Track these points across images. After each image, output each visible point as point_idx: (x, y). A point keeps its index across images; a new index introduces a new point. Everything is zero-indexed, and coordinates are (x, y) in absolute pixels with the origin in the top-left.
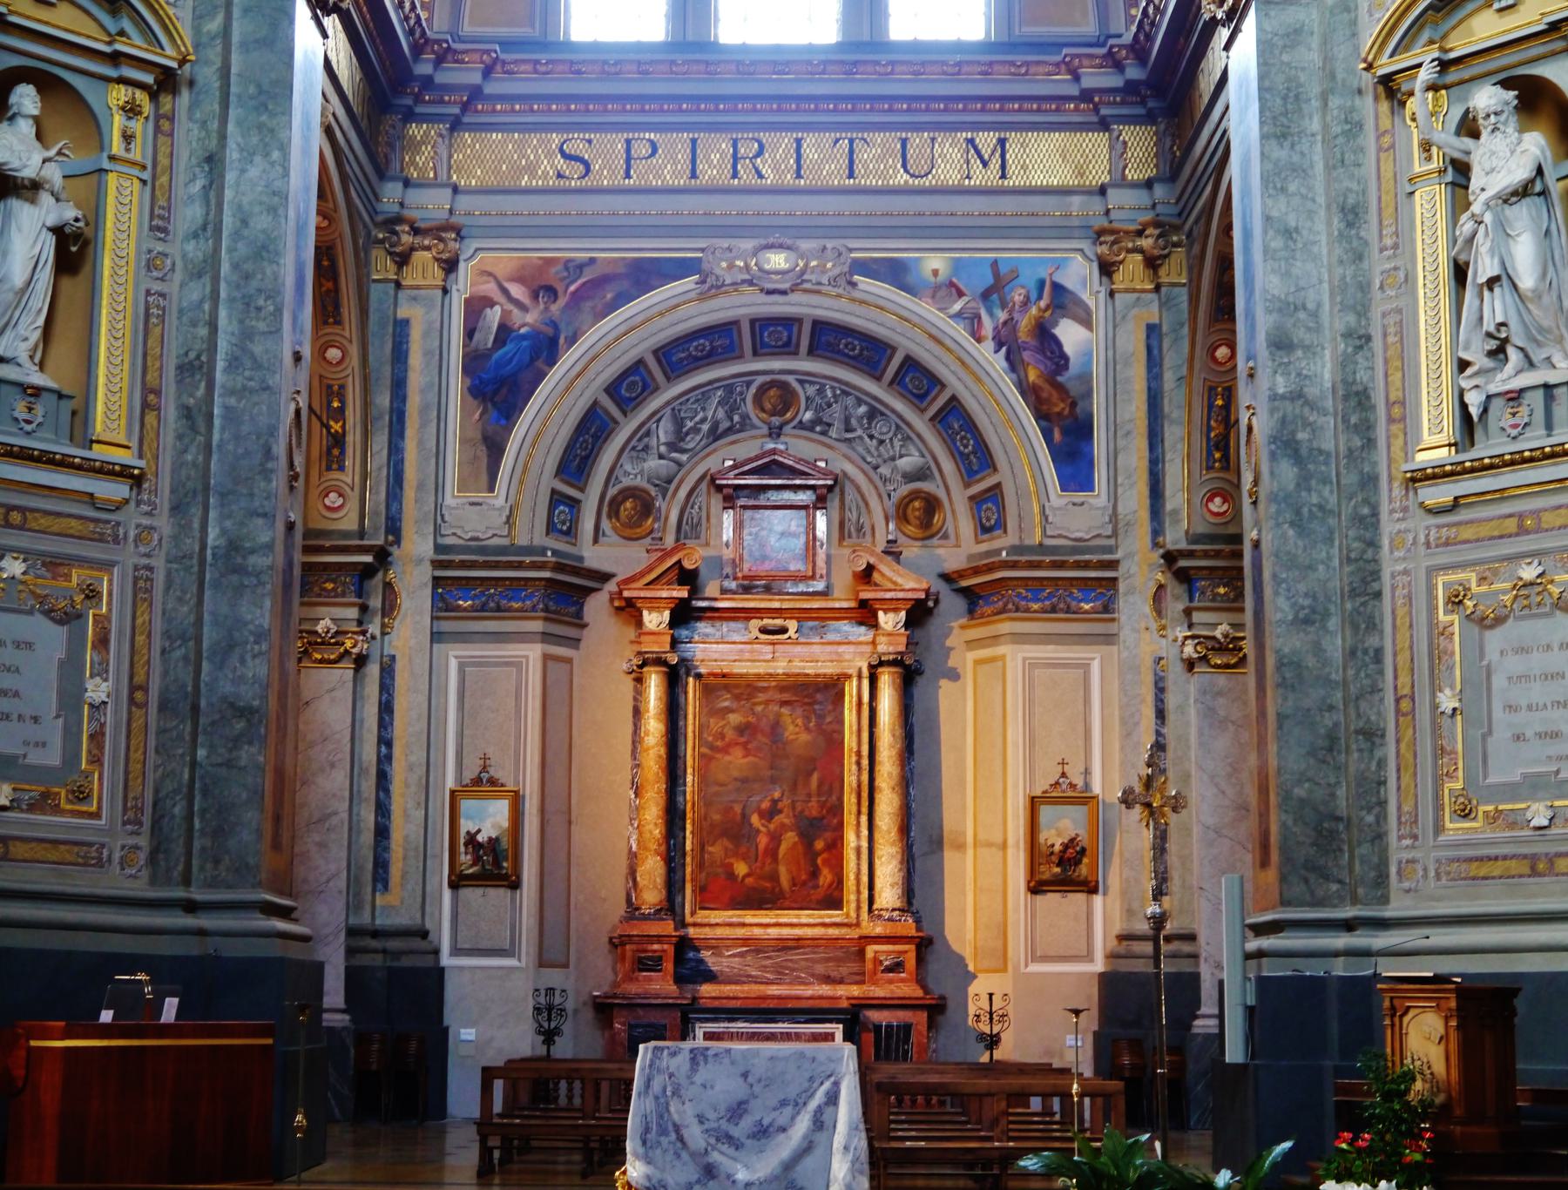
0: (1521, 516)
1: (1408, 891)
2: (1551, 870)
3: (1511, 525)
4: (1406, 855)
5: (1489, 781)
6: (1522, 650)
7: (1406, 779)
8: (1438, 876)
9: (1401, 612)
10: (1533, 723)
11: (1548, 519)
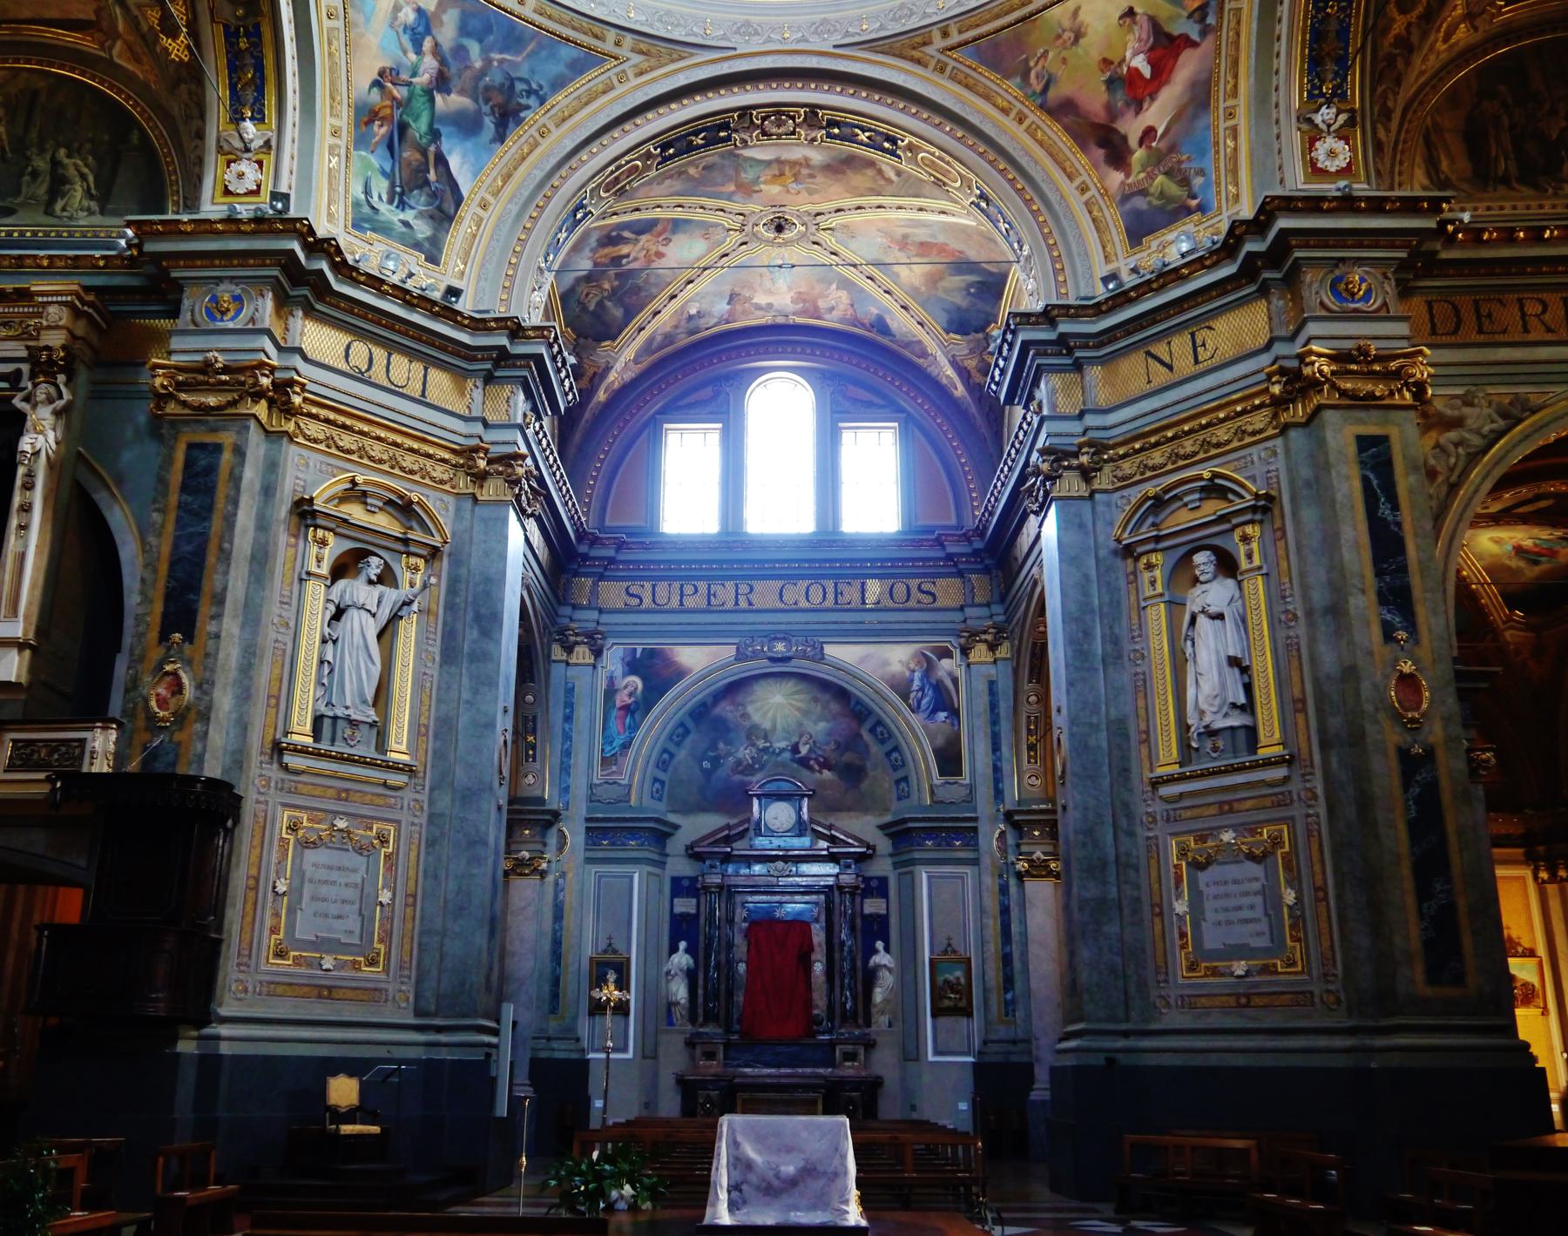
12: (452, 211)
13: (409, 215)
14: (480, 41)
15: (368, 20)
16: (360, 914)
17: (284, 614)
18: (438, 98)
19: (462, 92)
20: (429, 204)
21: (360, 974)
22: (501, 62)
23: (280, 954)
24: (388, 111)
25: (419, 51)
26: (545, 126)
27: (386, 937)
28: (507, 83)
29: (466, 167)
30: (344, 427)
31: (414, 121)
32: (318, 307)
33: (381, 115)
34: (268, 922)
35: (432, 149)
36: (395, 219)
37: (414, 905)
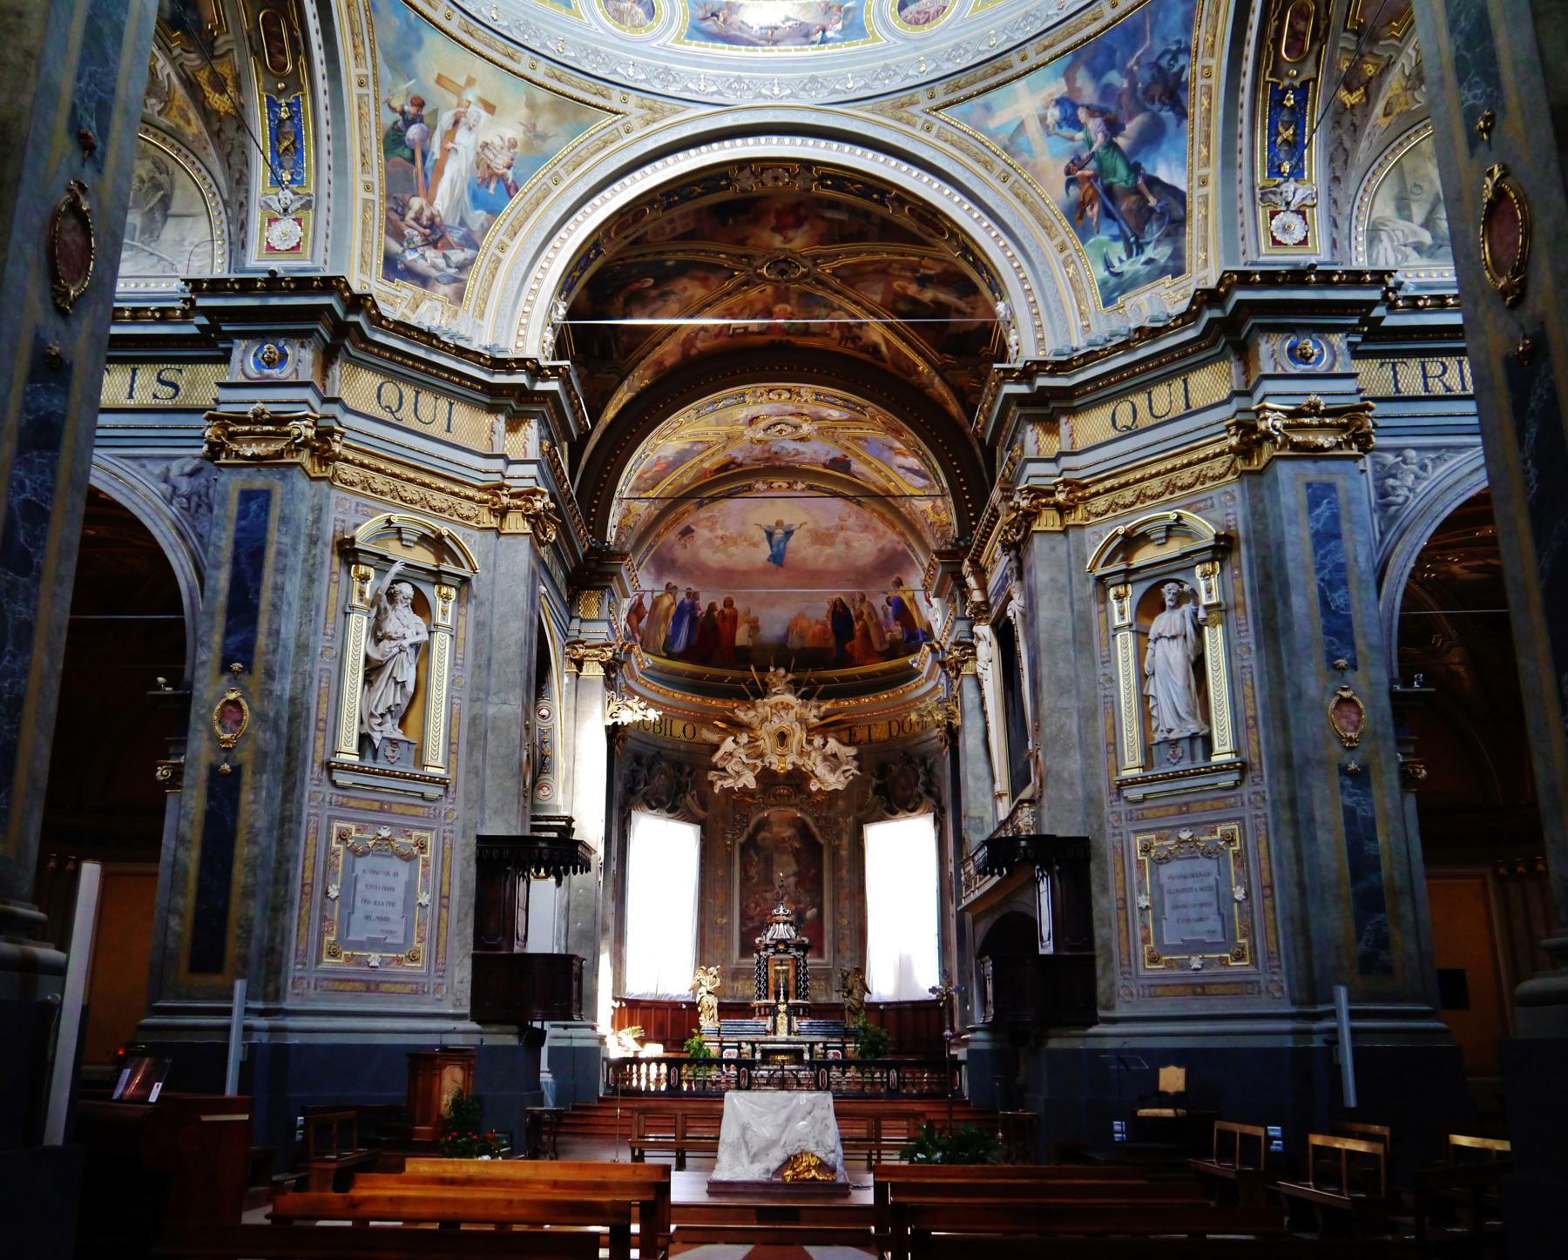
0: (382, 803)
1: (297, 995)
2: (377, 990)
3: (376, 806)
4: (298, 974)
5: (350, 938)
6: (375, 872)
7: (303, 930)
8: (316, 987)
9: (311, 837)
10: (376, 911)
11: (395, 808)
12: (1182, 213)
13: (1149, 252)
14: (1112, 67)
15: (1030, 152)
16: (1220, 914)
17: (1107, 671)
18: (1121, 141)
19: (1131, 117)
20: (1160, 227)
21: (1228, 970)
22: (1138, 62)
23: (1154, 960)
24: (1091, 192)
25: (1078, 125)
26: (1203, 67)
27: (1249, 932)
28: (1155, 70)
29: (1173, 167)
30: (1122, 486)
31: (1114, 176)
32: (1076, 403)
33: (1087, 199)
34: (1140, 934)
35: (1140, 181)
36: (1139, 266)
37: (1272, 895)
